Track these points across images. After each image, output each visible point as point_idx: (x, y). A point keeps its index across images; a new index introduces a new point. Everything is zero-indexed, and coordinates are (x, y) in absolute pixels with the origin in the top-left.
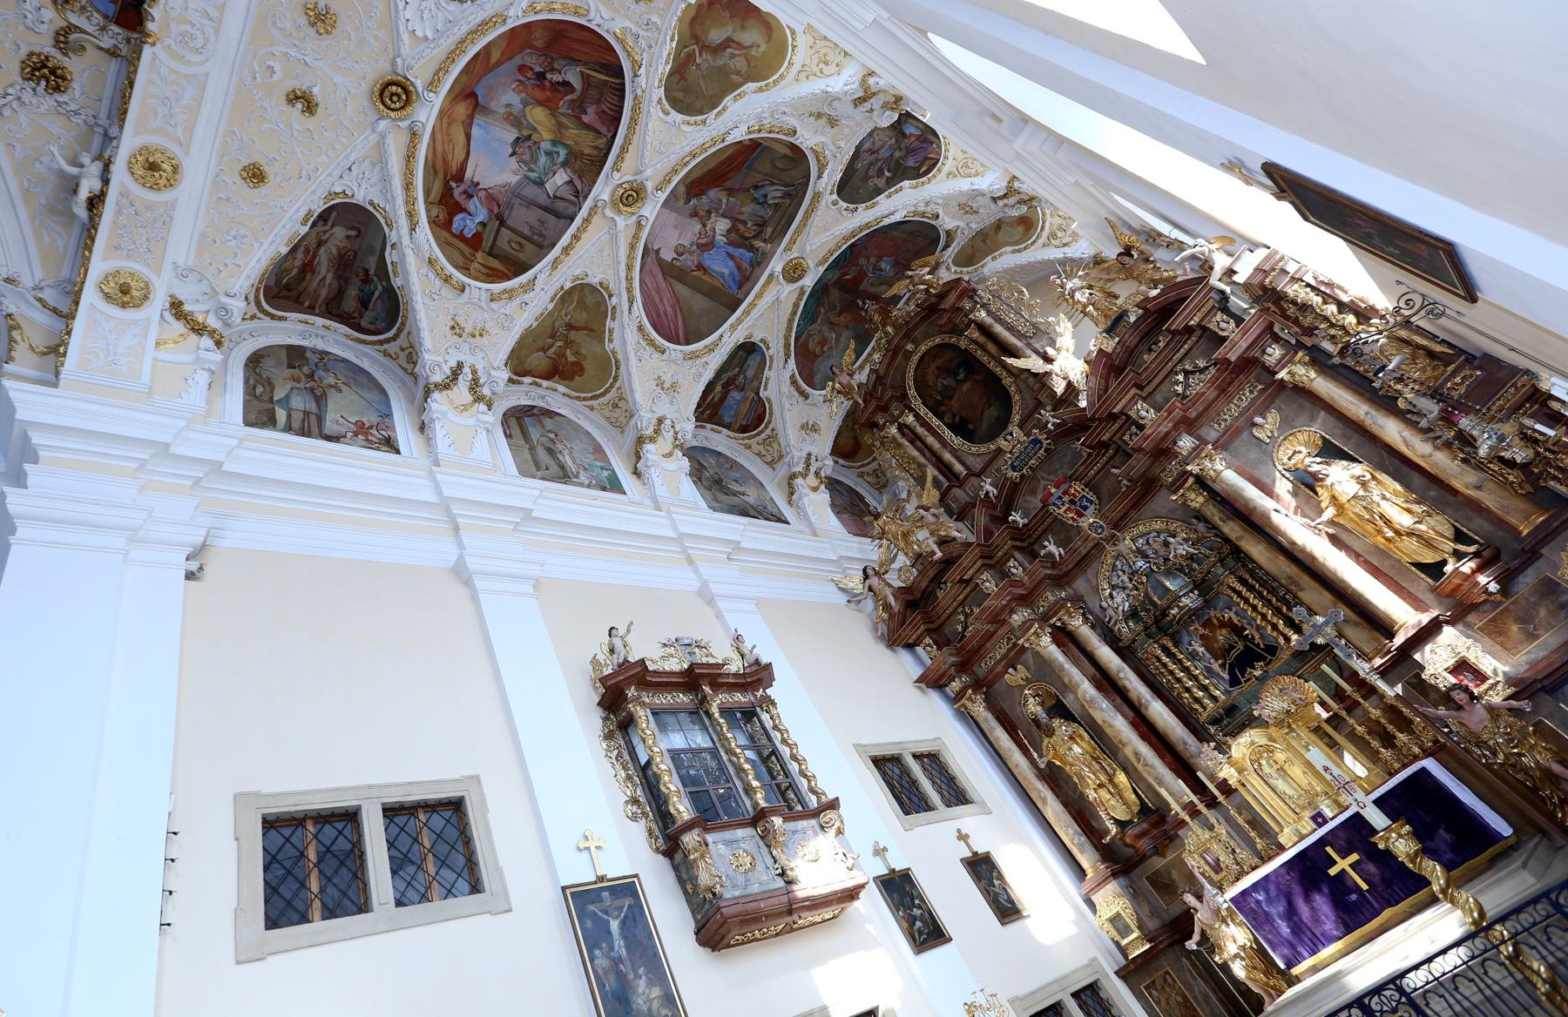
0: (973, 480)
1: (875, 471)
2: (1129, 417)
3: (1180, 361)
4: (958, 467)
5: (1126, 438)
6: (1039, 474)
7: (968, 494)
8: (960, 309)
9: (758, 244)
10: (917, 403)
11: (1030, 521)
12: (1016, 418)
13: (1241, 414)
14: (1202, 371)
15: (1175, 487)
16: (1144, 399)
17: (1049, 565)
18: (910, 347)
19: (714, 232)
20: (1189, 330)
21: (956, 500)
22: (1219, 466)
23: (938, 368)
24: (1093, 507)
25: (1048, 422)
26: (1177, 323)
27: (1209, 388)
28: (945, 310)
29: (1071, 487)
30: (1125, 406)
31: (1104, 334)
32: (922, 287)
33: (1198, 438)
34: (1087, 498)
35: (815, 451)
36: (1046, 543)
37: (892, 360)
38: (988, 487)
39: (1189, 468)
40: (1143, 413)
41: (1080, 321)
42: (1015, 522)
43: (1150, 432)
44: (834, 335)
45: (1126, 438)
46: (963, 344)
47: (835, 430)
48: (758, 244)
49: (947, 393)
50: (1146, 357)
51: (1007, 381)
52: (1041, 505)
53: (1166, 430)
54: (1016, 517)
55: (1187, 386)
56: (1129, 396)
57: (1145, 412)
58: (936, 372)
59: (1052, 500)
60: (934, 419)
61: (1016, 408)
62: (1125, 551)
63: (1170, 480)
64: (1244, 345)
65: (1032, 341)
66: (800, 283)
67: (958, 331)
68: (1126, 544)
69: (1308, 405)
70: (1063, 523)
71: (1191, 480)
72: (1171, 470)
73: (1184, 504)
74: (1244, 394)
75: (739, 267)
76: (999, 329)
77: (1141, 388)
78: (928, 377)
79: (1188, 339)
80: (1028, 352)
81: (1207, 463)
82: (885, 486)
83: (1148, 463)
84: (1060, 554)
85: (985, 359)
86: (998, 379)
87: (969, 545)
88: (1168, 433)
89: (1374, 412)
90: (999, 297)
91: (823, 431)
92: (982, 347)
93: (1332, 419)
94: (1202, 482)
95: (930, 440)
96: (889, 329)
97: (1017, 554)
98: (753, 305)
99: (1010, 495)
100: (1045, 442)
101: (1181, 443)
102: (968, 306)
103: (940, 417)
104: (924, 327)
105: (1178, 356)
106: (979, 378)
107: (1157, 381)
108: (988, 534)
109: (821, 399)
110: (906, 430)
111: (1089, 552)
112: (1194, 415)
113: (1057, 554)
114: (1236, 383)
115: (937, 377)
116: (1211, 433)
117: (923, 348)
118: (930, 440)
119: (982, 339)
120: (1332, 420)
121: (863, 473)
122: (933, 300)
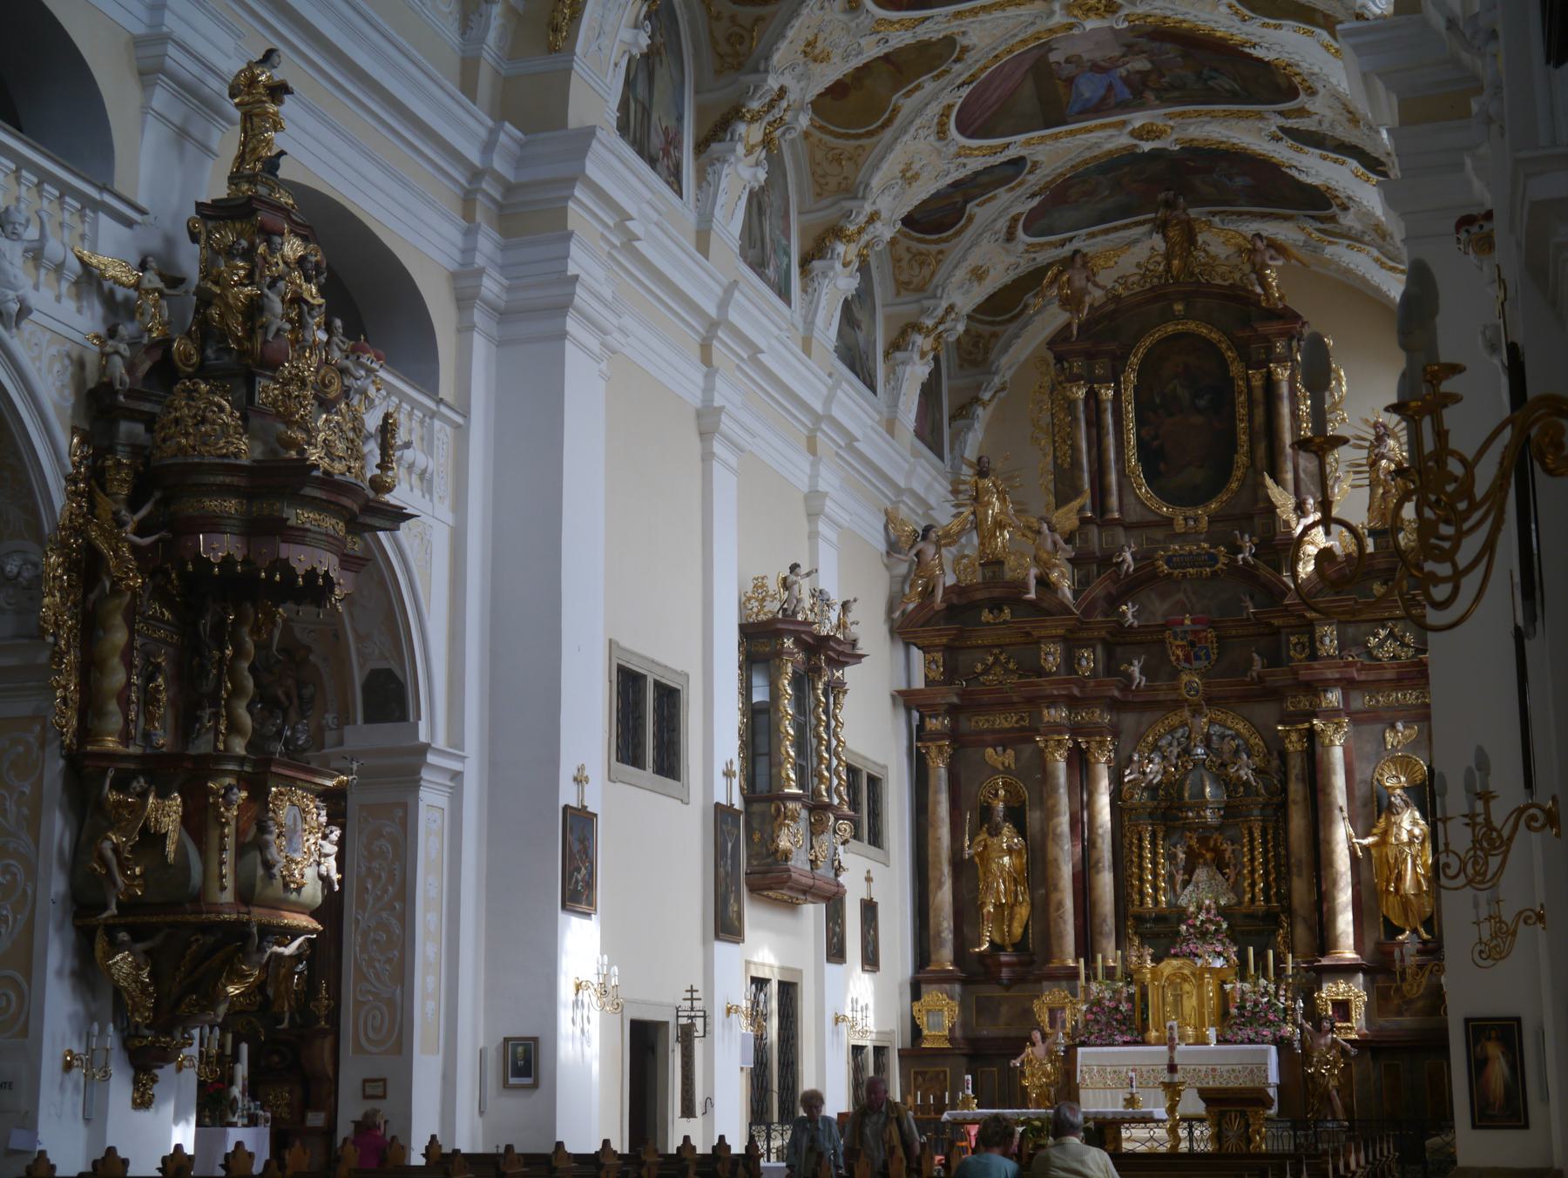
0: (1120, 531)
1: (979, 336)
4: (1114, 501)
9: (1150, 96)
11: (1139, 626)
14: (1403, 645)
18: (1178, 307)
19: (1124, 64)
22: (1338, 741)
24: (1206, 663)
25: (1240, 550)
36: (1136, 662)
38: (1128, 556)
40: (1327, 640)
42: (1124, 613)
44: (1106, 193)
45: (1294, 639)
46: (1236, 369)
47: (998, 285)
48: (1150, 96)
52: (1160, 621)
53: (1330, 676)
54: (1128, 609)
55: (1381, 645)
57: (1329, 637)
59: (1179, 629)
66: (1142, 143)
71: (1307, 725)
72: (1299, 702)
75: (1103, 99)
76: (1286, 409)
81: (1332, 728)
86: (1233, 447)
87: (1070, 612)
91: (989, 278)
92: (1251, 402)
94: (1312, 734)
95: (1111, 441)
96: (1176, 262)
98: (1071, 133)
99: (1142, 581)
100: (1219, 565)
101: (1329, 695)
102: (1279, 347)
103: (1140, 422)
109: (1021, 248)
110: (1092, 402)
112: (1363, 678)
116: (1360, 701)
117: (1192, 326)
118: (1111, 441)
119: (1259, 395)
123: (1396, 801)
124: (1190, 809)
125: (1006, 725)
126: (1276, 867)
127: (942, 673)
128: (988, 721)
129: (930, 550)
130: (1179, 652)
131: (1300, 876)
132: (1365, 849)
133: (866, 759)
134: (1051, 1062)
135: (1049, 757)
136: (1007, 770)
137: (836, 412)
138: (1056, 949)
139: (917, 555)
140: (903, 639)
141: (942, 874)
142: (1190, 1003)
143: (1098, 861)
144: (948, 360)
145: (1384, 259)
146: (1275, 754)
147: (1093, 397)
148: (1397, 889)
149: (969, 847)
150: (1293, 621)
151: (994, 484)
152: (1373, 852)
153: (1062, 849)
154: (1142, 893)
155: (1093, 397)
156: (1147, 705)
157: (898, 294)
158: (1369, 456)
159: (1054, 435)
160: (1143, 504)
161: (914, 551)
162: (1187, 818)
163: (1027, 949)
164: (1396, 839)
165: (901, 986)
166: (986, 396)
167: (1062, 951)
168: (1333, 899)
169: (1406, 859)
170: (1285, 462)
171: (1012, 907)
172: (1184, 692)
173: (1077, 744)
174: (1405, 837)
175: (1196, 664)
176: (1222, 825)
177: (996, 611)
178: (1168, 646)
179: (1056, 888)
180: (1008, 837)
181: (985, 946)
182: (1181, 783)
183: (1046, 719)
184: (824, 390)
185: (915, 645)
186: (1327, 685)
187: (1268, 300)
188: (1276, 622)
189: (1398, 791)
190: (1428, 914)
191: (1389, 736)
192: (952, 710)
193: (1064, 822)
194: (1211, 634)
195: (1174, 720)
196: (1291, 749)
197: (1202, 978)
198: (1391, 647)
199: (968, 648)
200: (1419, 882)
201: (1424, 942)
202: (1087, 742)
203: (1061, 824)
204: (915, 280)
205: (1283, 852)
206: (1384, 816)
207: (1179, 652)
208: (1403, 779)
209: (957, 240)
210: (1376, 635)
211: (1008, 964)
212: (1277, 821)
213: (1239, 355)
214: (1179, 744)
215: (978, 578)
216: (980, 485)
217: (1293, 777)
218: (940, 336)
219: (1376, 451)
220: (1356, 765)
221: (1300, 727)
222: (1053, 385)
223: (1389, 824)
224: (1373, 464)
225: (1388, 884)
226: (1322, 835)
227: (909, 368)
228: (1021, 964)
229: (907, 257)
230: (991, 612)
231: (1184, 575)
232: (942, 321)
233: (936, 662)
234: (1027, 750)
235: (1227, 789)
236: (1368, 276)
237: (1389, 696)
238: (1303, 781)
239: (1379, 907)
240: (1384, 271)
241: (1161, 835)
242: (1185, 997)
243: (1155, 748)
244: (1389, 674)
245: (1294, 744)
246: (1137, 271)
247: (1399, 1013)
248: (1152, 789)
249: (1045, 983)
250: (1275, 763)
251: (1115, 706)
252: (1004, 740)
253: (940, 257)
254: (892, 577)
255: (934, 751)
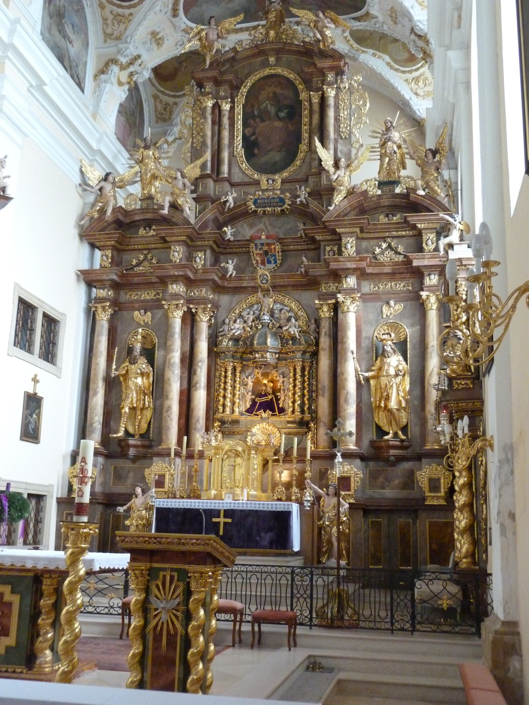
0: (226, 185)
1: (167, 104)
2: (340, 239)
3: (393, 237)
4: (225, 168)
5: (328, 248)
6: (265, 220)
7: (215, 189)
8: (324, 75)
10: (241, 99)
11: (234, 241)
12: (285, 174)
13: (389, 293)
14: (397, 253)
15: (324, 297)
16: (358, 238)
17: (220, 275)
18: (272, 60)
20: (414, 227)
21: (205, 187)
22: (353, 308)
23: (275, 93)
24: (274, 265)
25: (298, 196)
26: (412, 218)
27: (389, 266)
28: (315, 65)
29: (274, 244)
30: (345, 233)
31: (377, 183)
32: (319, 36)
33: (359, 284)
34: (276, 258)
35: (145, 56)
37: (254, 56)
38: (230, 199)
39: (339, 295)
40: (349, 246)
41: (375, 160)
42: (225, 232)
43: (341, 259)
45: (328, 248)
46: (303, 96)
49: (264, 116)
50: (382, 217)
51: (303, 147)
54: (228, 231)
55: (382, 253)
56: (352, 230)
58: (271, 95)
59: (258, 242)
60: (240, 122)
61: (291, 168)
62: (265, 304)
63: (324, 291)
64: (426, 262)
65: (340, 141)
67: (309, 86)
68: (269, 301)
69: (417, 317)
70: (249, 258)
71: (333, 301)
72: (330, 287)
73: (318, 309)
74: (400, 284)
76: (331, 113)
77: (362, 231)
78: (262, 92)
79: (409, 230)
80: (332, 146)
81: (348, 302)
82: (164, 120)
83: (324, 273)
84: (231, 275)
85: (305, 120)
86: (299, 140)
87: (188, 223)
88: (348, 269)
89: (436, 348)
90: (351, 93)
91: (165, 46)
93: (419, 334)
94: (336, 307)
95: (226, 134)
96: (272, 33)
97: (208, 252)
100: (286, 206)
101: (348, 280)
102: (330, 77)
104: (293, 58)
105: (395, 233)
106: (291, 127)
107: (372, 235)
108: (204, 226)
109: (183, 26)
110: (217, 111)
111: (247, 287)
112: (369, 270)
113: (230, 273)
114: (403, 276)
115: (268, 99)
116: (367, 287)
117: (279, 71)
119: (316, 107)
120: (417, 335)
121: (157, 96)
122: (316, 49)
123: (388, 348)
124: (257, 352)
125: (148, 297)
126: (310, 392)
127: (110, 263)
128: (137, 295)
129: (108, 187)
130: (258, 259)
131: (323, 396)
132: (367, 380)
133: (42, 302)
134: (146, 509)
135: (170, 315)
136: (146, 325)
137: (17, 42)
138: (164, 437)
139: (101, 189)
140: (89, 243)
141: (97, 387)
142: (240, 472)
143: (197, 383)
144: (150, 117)
145: (392, 63)
146: (313, 321)
147: (217, 107)
148: (386, 406)
149: (116, 370)
150: (329, 237)
151: (153, 154)
152: (372, 382)
153: (173, 372)
154: (224, 406)
155: (217, 107)
156: (237, 290)
157: (105, 41)
158: (381, 140)
159: (193, 130)
160: (244, 172)
161: (98, 187)
162: (255, 358)
163: (148, 438)
164: (387, 373)
165: (64, 457)
166: (170, 139)
167: (168, 438)
168: (345, 410)
169: (392, 386)
170: (329, 143)
171: (142, 410)
172: (259, 281)
173: (189, 309)
174: (392, 372)
175: (269, 266)
176: (277, 364)
177: (147, 228)
178: (252, 254)
179: (167, 397)
180: (143, 364)
181: (121, 434)
182: (253, 337)
183: (170, 292)
184: (8, 24)
185: (98, 248)
186: (347, 272)
187: (324, 45)
188: (318, 238)
189: (390, 343)
190: (405, 424)
191: (385, 309)
192: (116, 286)
193: (176, 357)
194: (278, 247)
195: (252, 299)
196: (323, 316)
197: (249, 454)
198: (389, 254)
199: (129, 250)
200: (400, 402)
201: (402, 441)
202: (197, 309)
203: (174, 357)
204: (116, 33)
205: (315, 383)
206: (379, 359)
207: (258, 259)
208: (393, 335)
209: (141, 6)
210: (380, 246)
211: (135, 446)
212: (312, 362)
213: (306, 87)
214: (254, 314)
215: (138, 207)
216: (145, 153)
217: (323, 334)
218: (131, 75)
219: (385, 137)
220: (363, 327)
221: (329, 302)
222: (195, 101)
223: (383, 363)
224: (383, 145)
225: (380, 402)
226: (339, 370)
227: (108, 86)
228: (143, 446)
229: (111, 17)
230: (145, 229)
231: (264, 211)
232: (131, 63)
233: (107, 256)
234: (159, 313)
235: (282, 343)
236: (383, 73)
237: (386, 285)
238: (330, 336)
239: (373, 418)
240: (392, 71)
241: (238, 369)
242: (237, 467)
243: (240, 316)
244: (387, 270)
245: (325, 313)
246: (249, 38)
247: (383, 488)
248: (236, 340)
249: (155, 459)
250: (313, 326)
251: (218, 289)
252: (146, 307)
253: (130, 17)
254: (85, 204)
255: (100, 310)
